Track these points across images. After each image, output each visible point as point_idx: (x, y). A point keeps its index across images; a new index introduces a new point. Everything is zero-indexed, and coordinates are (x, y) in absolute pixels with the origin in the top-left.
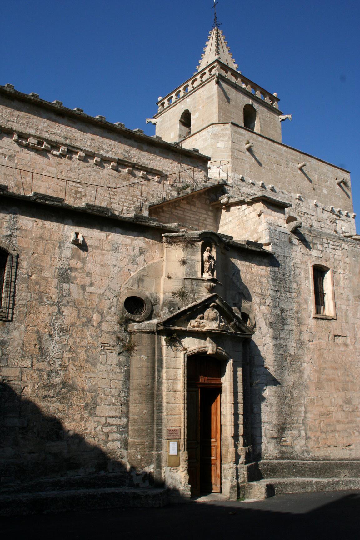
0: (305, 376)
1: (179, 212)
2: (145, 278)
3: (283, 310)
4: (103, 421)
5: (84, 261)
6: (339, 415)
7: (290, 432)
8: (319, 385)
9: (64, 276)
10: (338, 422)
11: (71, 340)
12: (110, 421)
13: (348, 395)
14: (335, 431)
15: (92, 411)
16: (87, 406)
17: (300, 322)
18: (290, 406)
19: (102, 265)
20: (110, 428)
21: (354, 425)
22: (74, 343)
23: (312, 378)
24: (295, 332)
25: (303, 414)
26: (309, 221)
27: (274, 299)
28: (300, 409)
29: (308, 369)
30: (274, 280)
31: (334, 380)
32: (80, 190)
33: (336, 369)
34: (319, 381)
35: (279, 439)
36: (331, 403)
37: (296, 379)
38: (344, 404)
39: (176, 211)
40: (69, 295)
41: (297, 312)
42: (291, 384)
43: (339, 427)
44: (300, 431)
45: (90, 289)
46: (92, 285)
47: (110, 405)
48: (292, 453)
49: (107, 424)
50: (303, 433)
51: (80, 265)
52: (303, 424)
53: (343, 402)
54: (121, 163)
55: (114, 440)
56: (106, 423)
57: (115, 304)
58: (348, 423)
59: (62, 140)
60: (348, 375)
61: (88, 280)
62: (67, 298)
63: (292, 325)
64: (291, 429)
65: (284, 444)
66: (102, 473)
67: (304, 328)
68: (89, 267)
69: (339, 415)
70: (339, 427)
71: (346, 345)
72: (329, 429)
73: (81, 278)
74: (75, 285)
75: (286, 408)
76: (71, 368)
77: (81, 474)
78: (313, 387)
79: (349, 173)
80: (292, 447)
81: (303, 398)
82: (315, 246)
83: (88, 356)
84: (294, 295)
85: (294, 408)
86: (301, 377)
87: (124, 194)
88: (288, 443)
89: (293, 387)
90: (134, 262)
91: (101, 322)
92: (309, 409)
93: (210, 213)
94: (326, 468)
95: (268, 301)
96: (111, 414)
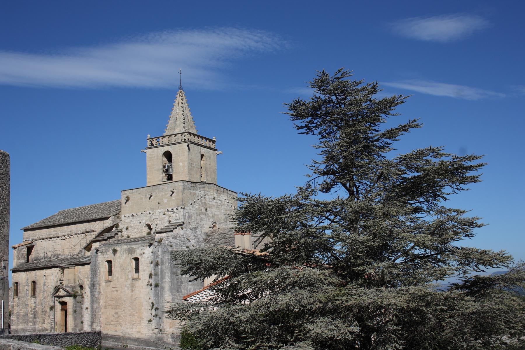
3: (94, 282)
6: (112, 319)
8: (105, 308)
9: (44, 285)
10: (112, 321)
13: (117, 311)
17: (100, 285)
18: (95, 315)
26: (156, 223)
27: (91, 278)
29: (102, 302)
34: (105, 306)
35: (91, 326)
54: (83, 233)
63: (97, 286)
64: (95, 323)
67: (101, 287)
69: (112, 319)
70: (112, 323)
71: (117, 291)
72: (108, 323)
78: (103, 308)
89: (96, 308)
90: (56, 277)
95: (90, 280)
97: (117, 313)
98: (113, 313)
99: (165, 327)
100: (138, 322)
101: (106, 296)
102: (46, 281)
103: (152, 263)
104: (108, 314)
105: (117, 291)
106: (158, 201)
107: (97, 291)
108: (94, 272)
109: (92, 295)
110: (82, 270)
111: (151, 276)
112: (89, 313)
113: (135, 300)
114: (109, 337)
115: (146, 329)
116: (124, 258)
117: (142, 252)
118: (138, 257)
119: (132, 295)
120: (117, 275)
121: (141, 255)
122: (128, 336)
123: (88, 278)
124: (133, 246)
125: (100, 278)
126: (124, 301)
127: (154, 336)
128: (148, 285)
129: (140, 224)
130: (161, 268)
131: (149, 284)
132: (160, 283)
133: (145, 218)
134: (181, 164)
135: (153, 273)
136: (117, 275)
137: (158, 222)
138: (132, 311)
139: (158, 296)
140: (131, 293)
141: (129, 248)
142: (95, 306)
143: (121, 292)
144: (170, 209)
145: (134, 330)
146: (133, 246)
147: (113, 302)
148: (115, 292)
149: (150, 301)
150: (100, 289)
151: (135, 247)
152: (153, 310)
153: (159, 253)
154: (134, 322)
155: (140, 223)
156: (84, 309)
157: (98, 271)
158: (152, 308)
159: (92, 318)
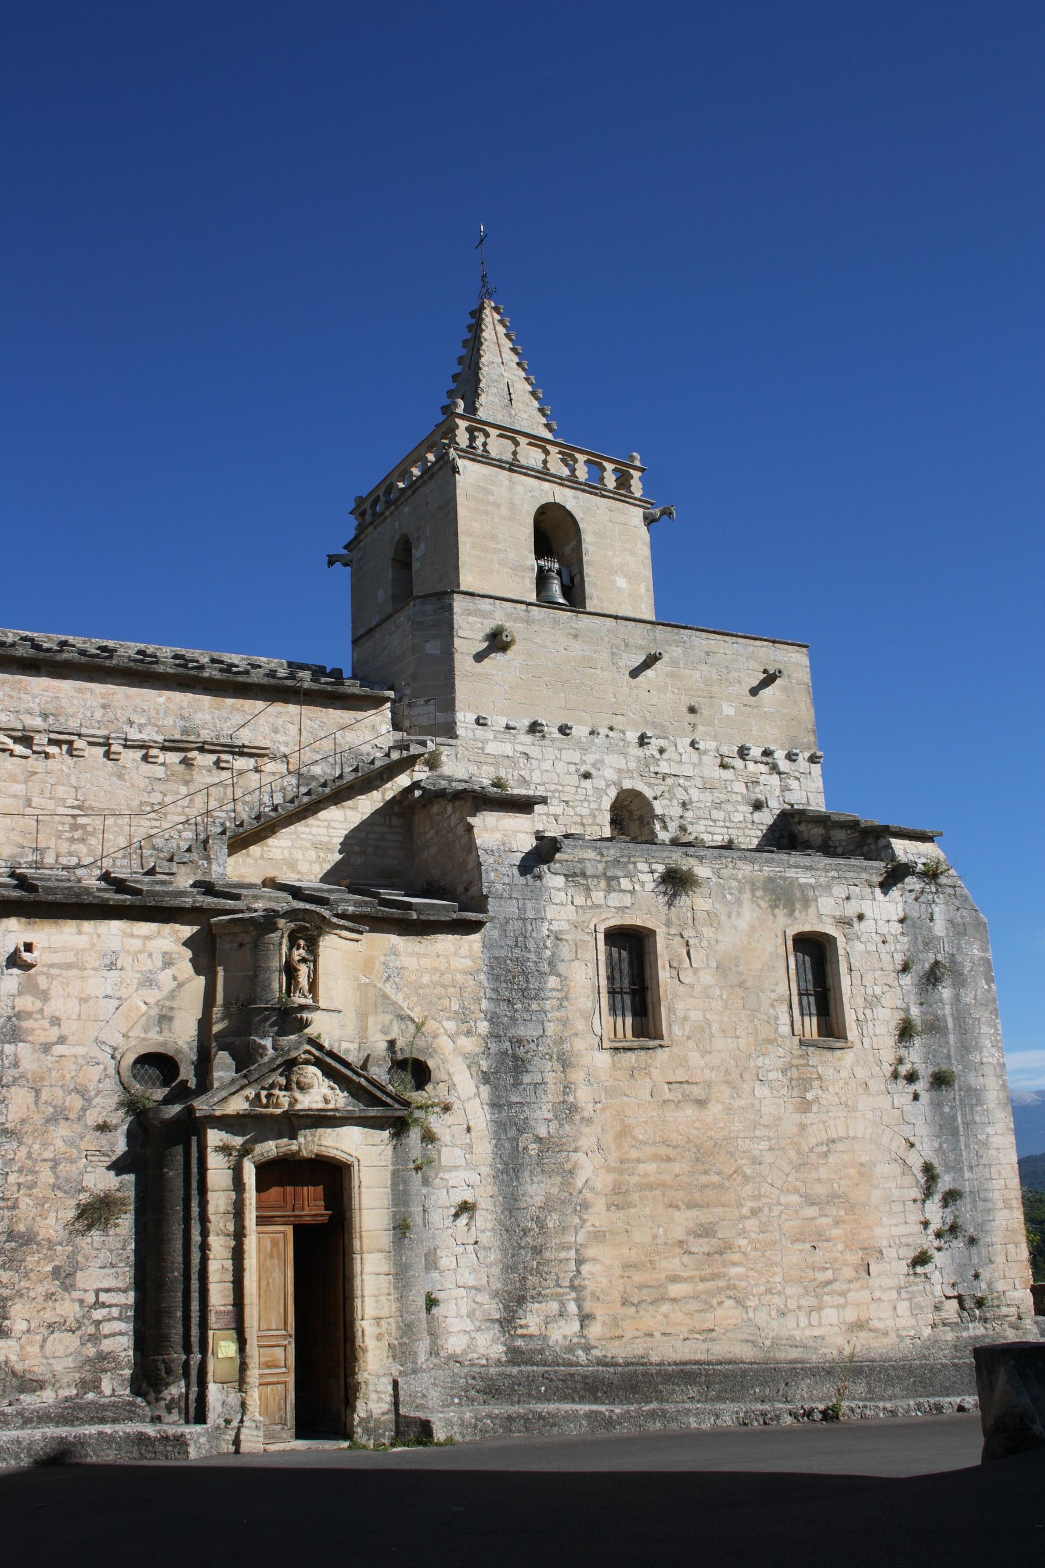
0: (579, 1183)
1: (314, 830)
2: (176, 1013)
4: (91, 1299)
5: (44, 996)
6: (673, 1264)
7: (536, 1305)
8: (619, 1198)
10: (674, 1279)
11: (23, 1151)
12: (103, 1297)
14: (663, 1299)
15: (68, 1281)
16: (56, 1272)
17: (565, 1062)
18: (537, 1251)
19: (81, 999)
20: (104, 1311)
21: (722, 1283)
22: (29, 1155)
23: (599, 1186)
24: (551, 1087)
25: (573, 1266)
26: (681, 795)
27: (493, 1019)
28: (563, 1255)
29: (590, 1170)
30: (496, 978)
31: (663, 1185)
32: (81, 821)
33: (668, 1159)
35: (508, 1322)
36: (655, 1237)
37: (554, 1191)
38: (691, 1238)
39: (307, 830)
40: (16, 1065)
41: (561, 1040)
42: (539, 1200)
43: (675, 1290)
44: (562, 1304)
45: (58, 1050)
46: (62, 1040)
47: (104, 1267)
48: (541, 1351)
49: (98, 1304)
50: (572, 1308)
51: (39, 1004)
52: (572, 1287)
53: (688, 1233)
54: (170, 746)
55: (114, 1335)
56: (97, 1301)
57: (112, 1071)
58: (703, 1279)
59: (38, 722)
60: (706, 1172)
61: (54, 1033)
62: (13, 1072)
64: (539, 1297)
65: (520, 1331)
66: (90, 1396)
67: (577, 1076)
68: (56, 1006)
69: (673, 1264)
70: (675, 1290)
72: (645, 1295)
73: (40, 1030)
74: (28, 1045)
75: (527, 1256)
76: (25, 1202)
77: (48, 1396)
78: (599, 1205)
79: (806, 647)
80: (545, 1338)
81: (572, 1232)
82: (614, 883)
83: (57, 1177)
84: (548, 1005)
85: (547, 1255)
86: (566, 1184)
87: (182, 814)
88: (533, 1330)
89: (547, 1207)
91: (84, 1110)
92: (589, 1253)
93: (395, 821)
94: (638, 1381)
95: (483, 1027)
96: (106, 1285)
97: (705, 1231)
98: (679, 1234)
99: (1000, 1286)
100: (848, 1272)
101: (623, 1133)
102: (26, 1003)
103: (905, 968)
104: (640, 1236)
105: (701, 1103)
106: (686, 701)
107: (550, 1096)
108: (515, 982)
109: (509, 1123)
110: (410, 963)
111: (905, 1032)
112: (485, 1238)
113: (825, 1155)
114: (668, 1378)
115: (903, 1307)
116: (743, 924)
117: (851, 910)
118: (830, 930)
119: (803, 1127)
120: (696, 1016)
121: (845, 922)
122: (794, 1354)
123: (463, 1016)
124: (791, 873)
125: (565, 1022)
126: (756, 1161)
127: (950, 1336)
128: (895, 1076)
129: (587, 783)
130: (957, 998)
131: (903, 1070)
132: (957, 1068)
133: (613, 760)
134: (621, 582)
135: (918, 1022)
136: (696, 1016)
137: (695, 794)
138: (811, 1211)
139: (955, 1132)
140: (797, 1117)
141: (770, 880)
142: (536, 1191)
143: (728, 1110)
144: (756, 752)
145: (830, 1315)
146: (791, 873)
147: (677, 1168)
148: (690, 1111)
149: (916, 1162)
150: (567, 1088)
151: (805, 878)
152: (934, 1211)
153: (939, 928)
154: (829, 1274)
155: (587, 776)
156: (441, 1217)
157: (553, 982)
158: (928, 1193)
159: (509, 1268)
